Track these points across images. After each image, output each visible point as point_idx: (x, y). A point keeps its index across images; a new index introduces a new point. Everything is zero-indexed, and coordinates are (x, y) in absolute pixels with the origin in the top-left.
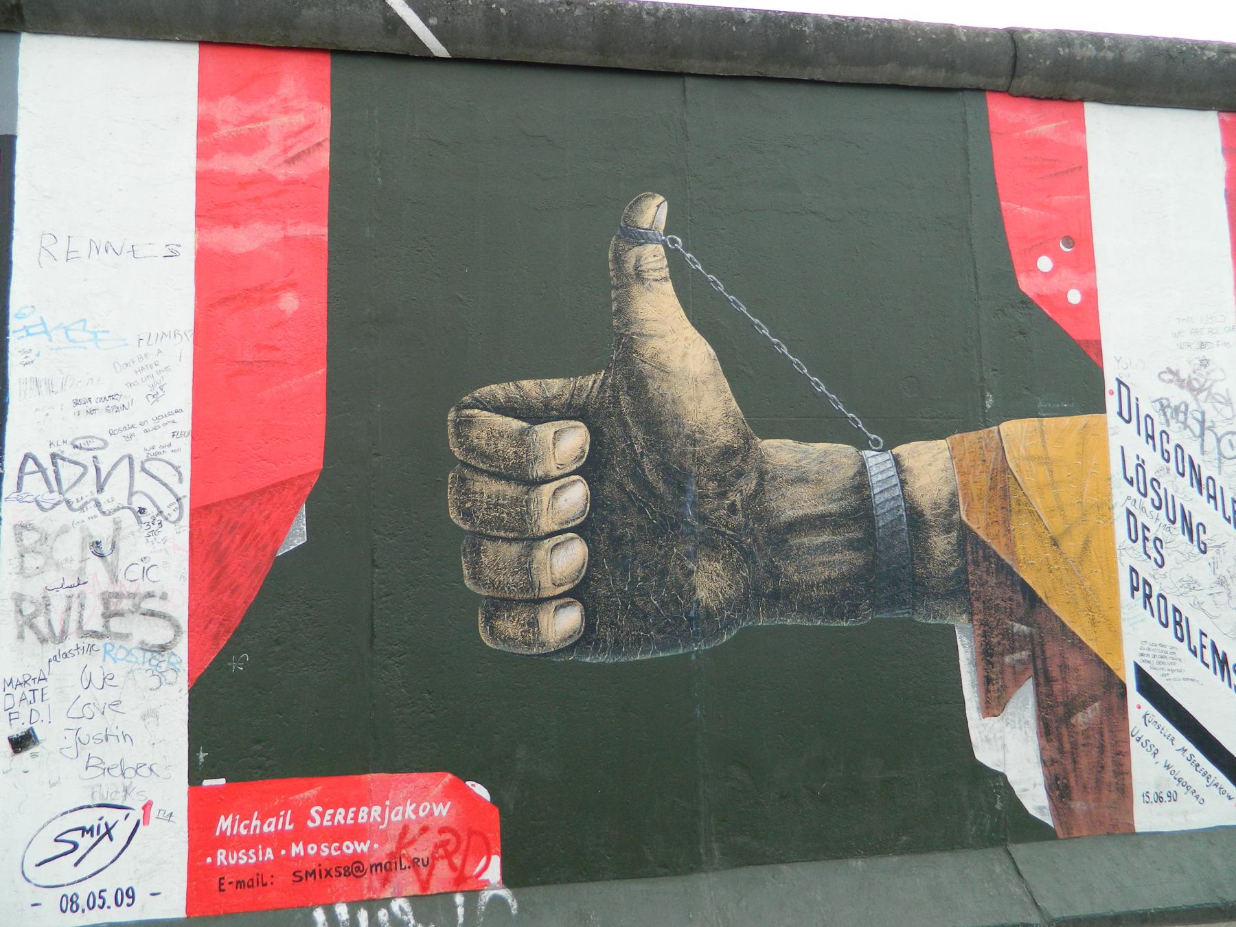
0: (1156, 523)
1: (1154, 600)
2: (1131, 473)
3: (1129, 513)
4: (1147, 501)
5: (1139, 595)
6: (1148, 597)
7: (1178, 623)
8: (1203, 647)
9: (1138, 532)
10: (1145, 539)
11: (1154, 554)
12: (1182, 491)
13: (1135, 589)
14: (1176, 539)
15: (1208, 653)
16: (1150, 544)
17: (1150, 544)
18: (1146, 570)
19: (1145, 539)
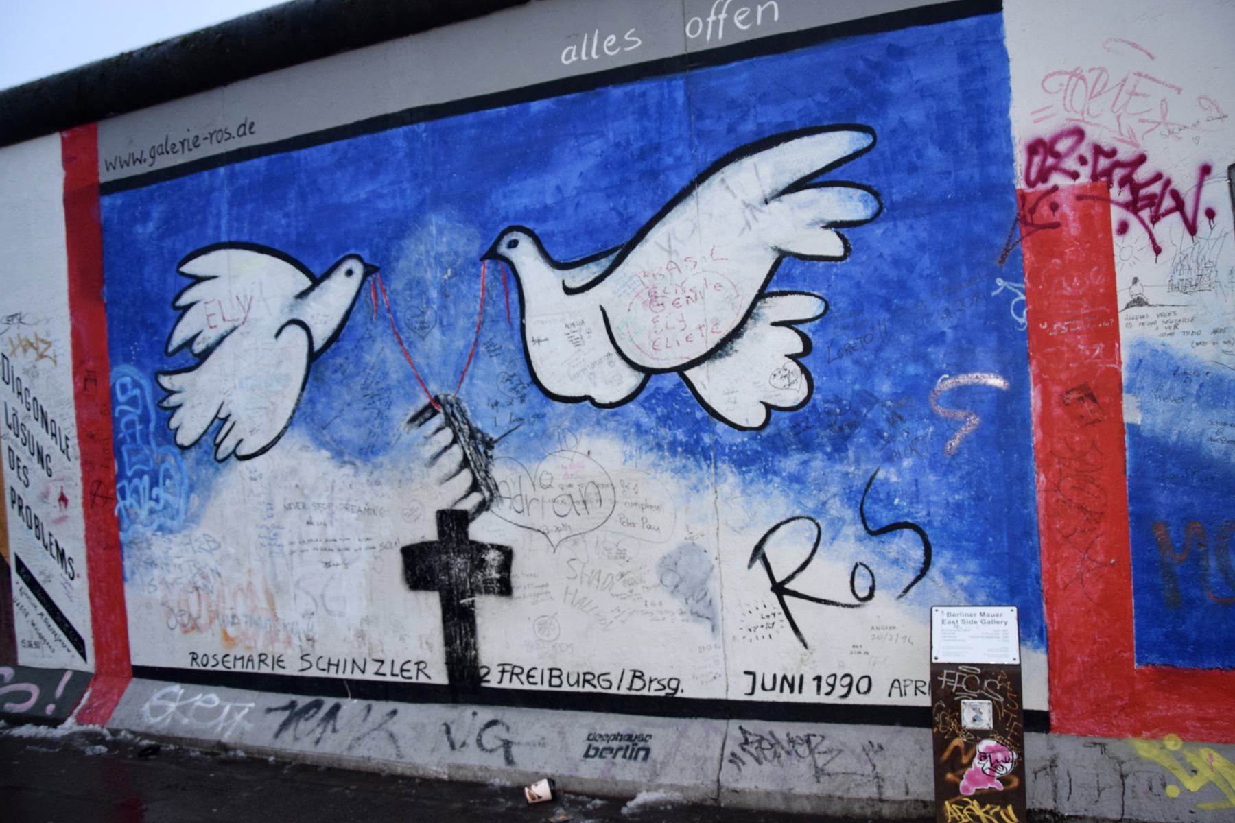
0: (23, 453)
1: (24, 510)
2: (10, 421)
3: (10, 449)
4: (19, 440)
5: (16, 506)
6: (20, 508)
7: (37, 527)
8: (51, 544)
9: (15, 463)
10: (19, 467)
11: (23, 478)
12: (35, 428)
13: (14, 502)
14: (34, 464)
15: (54, 548)
16: (21, 471)
17: (21, 471)
18: (20, 489)
19: (19, 467)
